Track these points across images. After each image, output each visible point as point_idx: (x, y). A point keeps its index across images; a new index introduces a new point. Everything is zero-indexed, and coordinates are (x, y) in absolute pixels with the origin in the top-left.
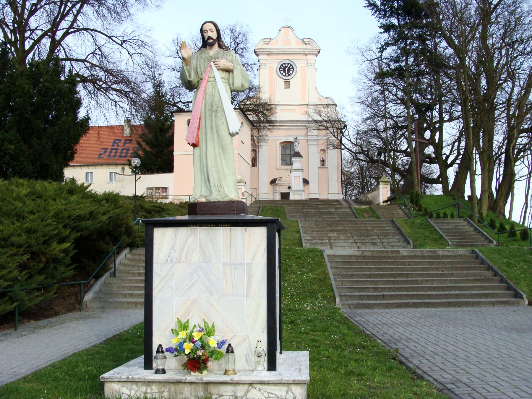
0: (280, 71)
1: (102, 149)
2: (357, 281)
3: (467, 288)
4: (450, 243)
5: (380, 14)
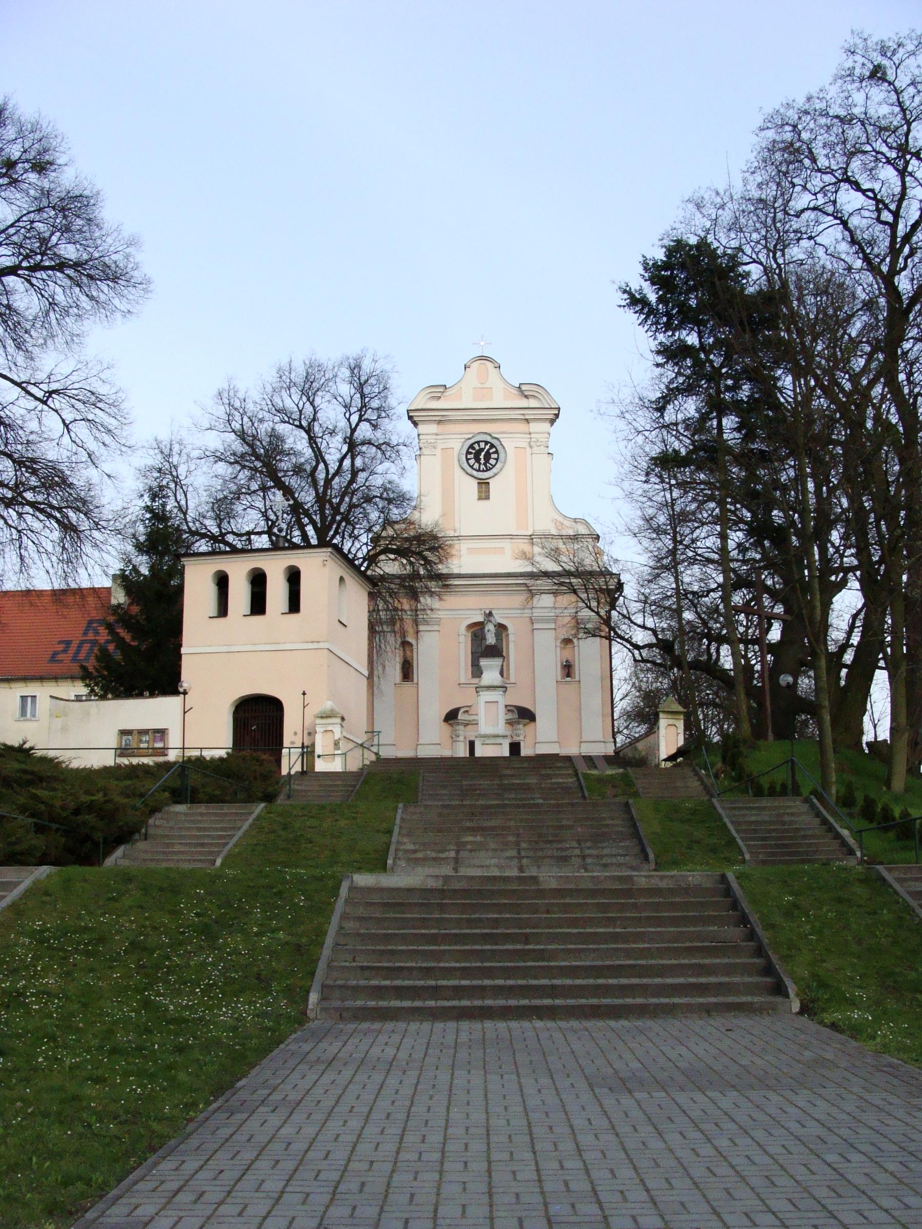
0: (467, 460)
1: (60, 642)
2: (392, 952)
3: (662, 971)
4: (747, 857)
5: (657, 323)
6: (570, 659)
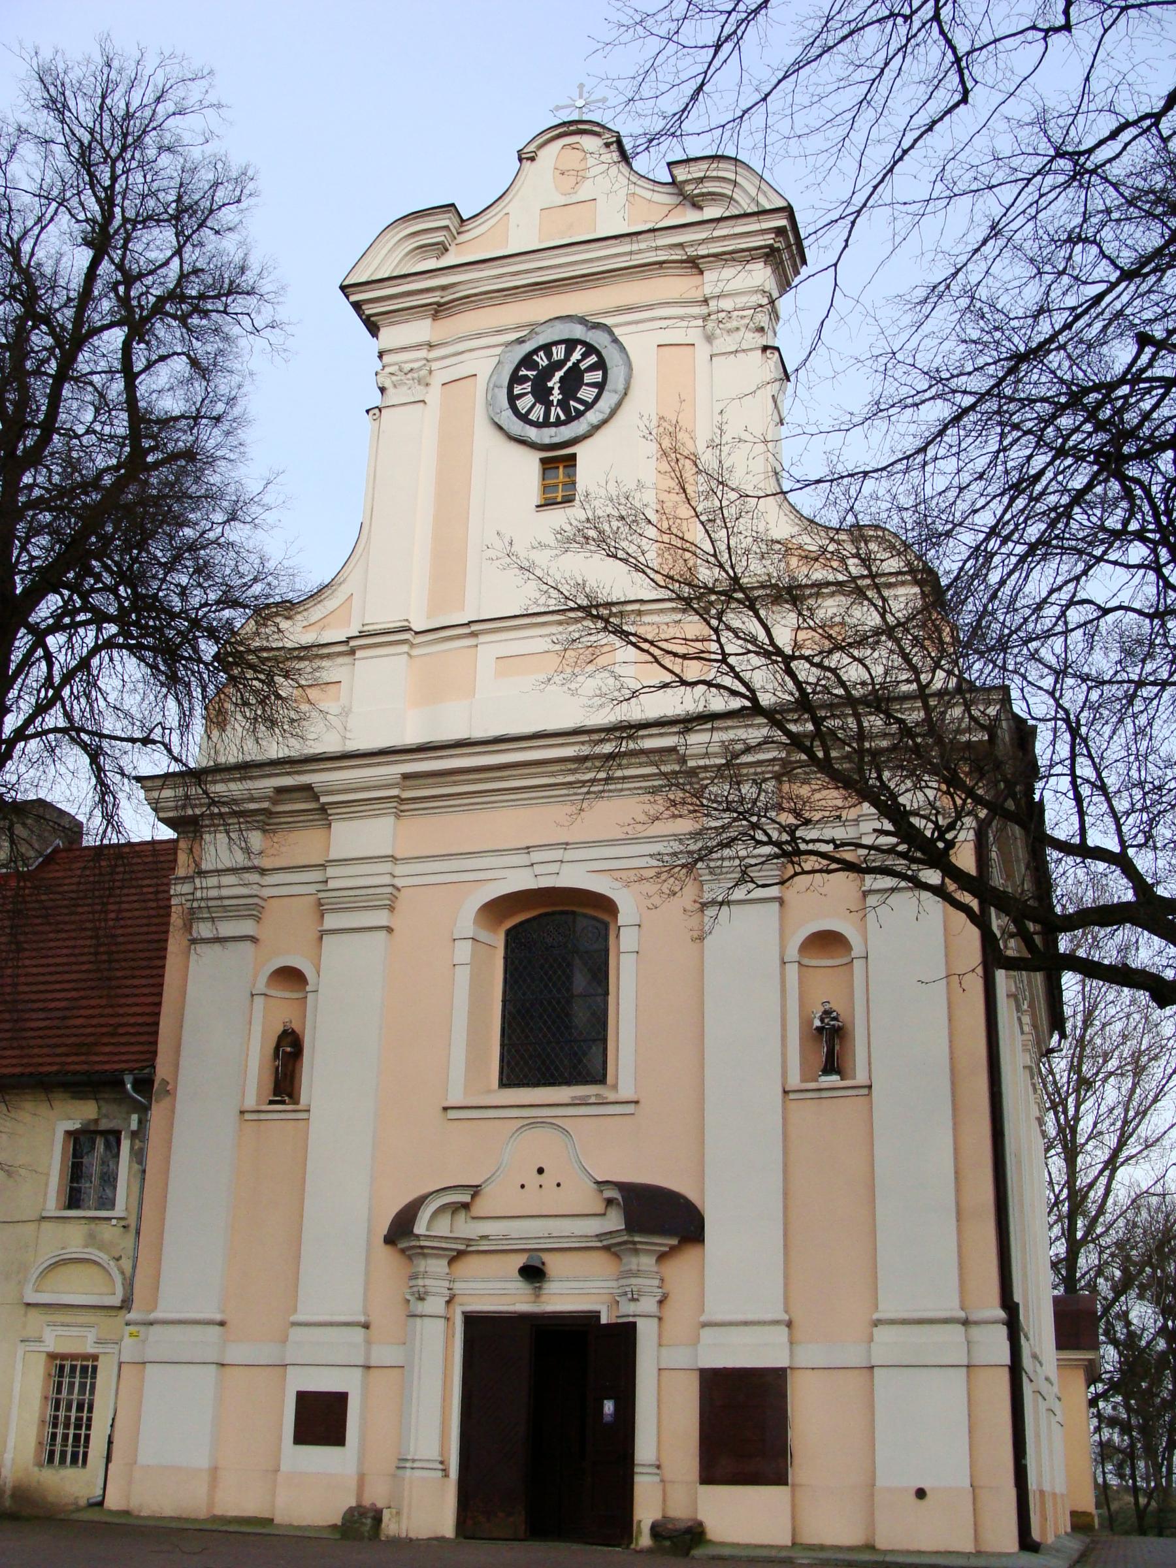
0: (512, 399)
6: (837, 1006)
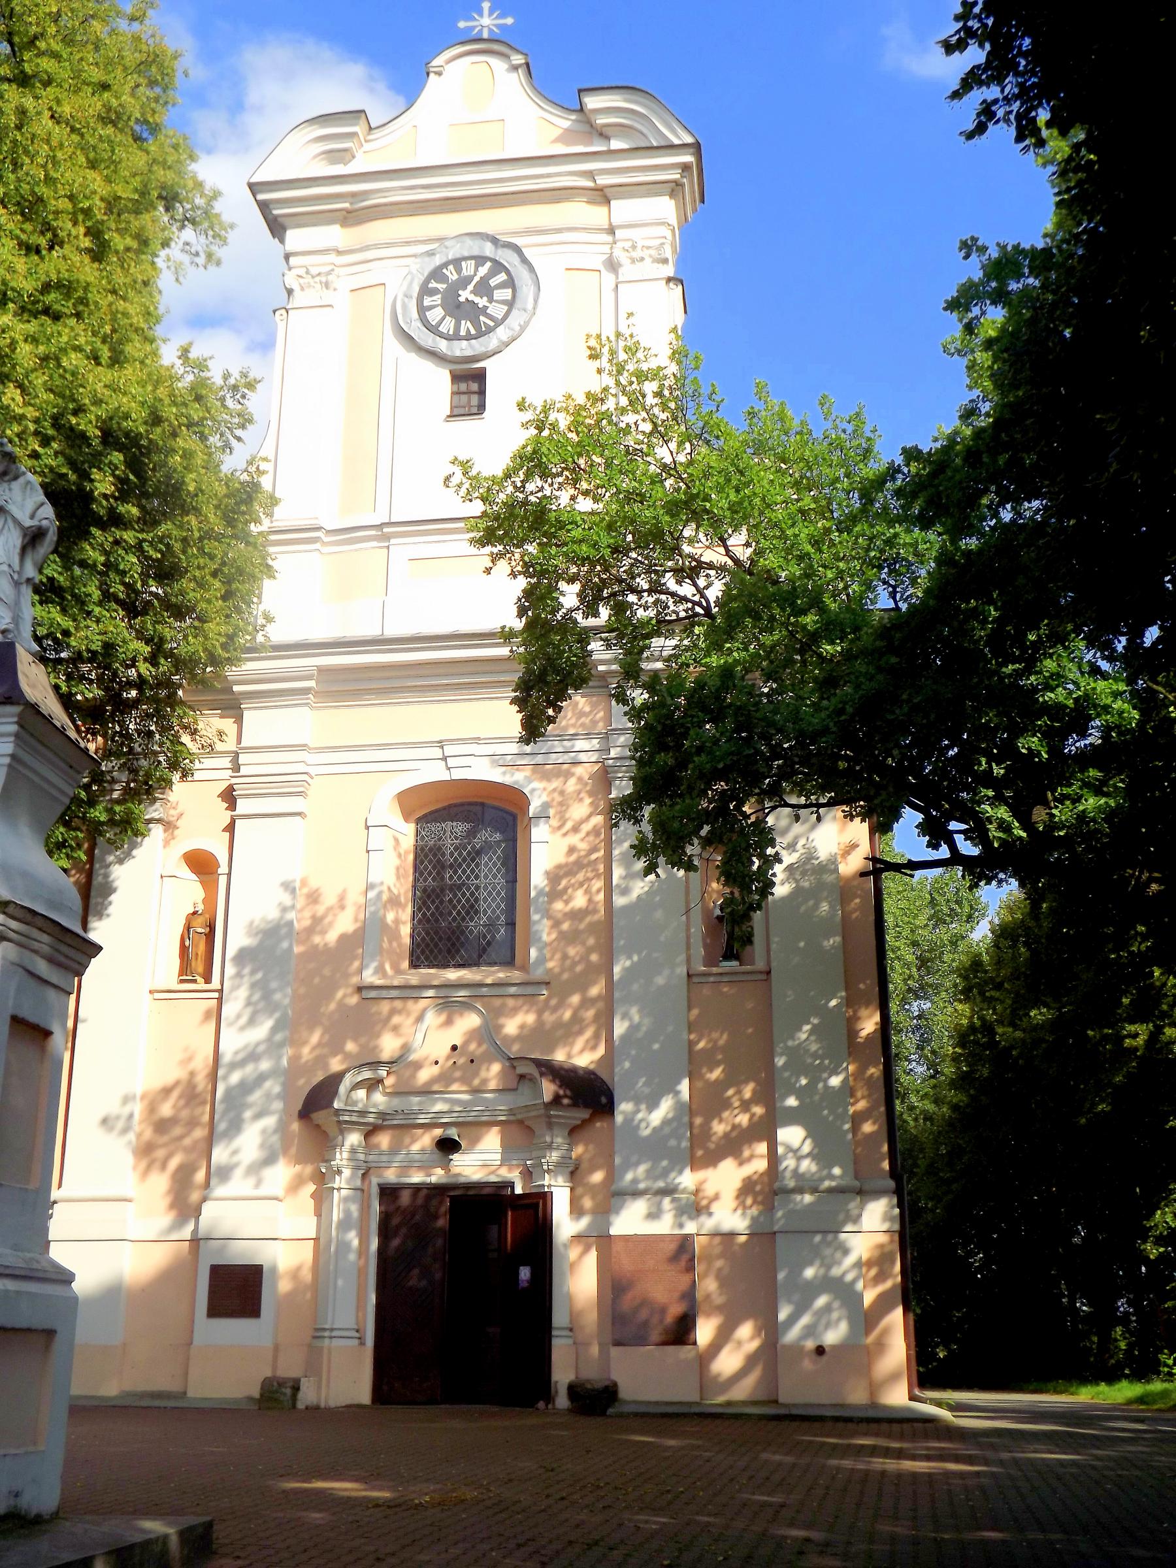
0: (422, 310)
